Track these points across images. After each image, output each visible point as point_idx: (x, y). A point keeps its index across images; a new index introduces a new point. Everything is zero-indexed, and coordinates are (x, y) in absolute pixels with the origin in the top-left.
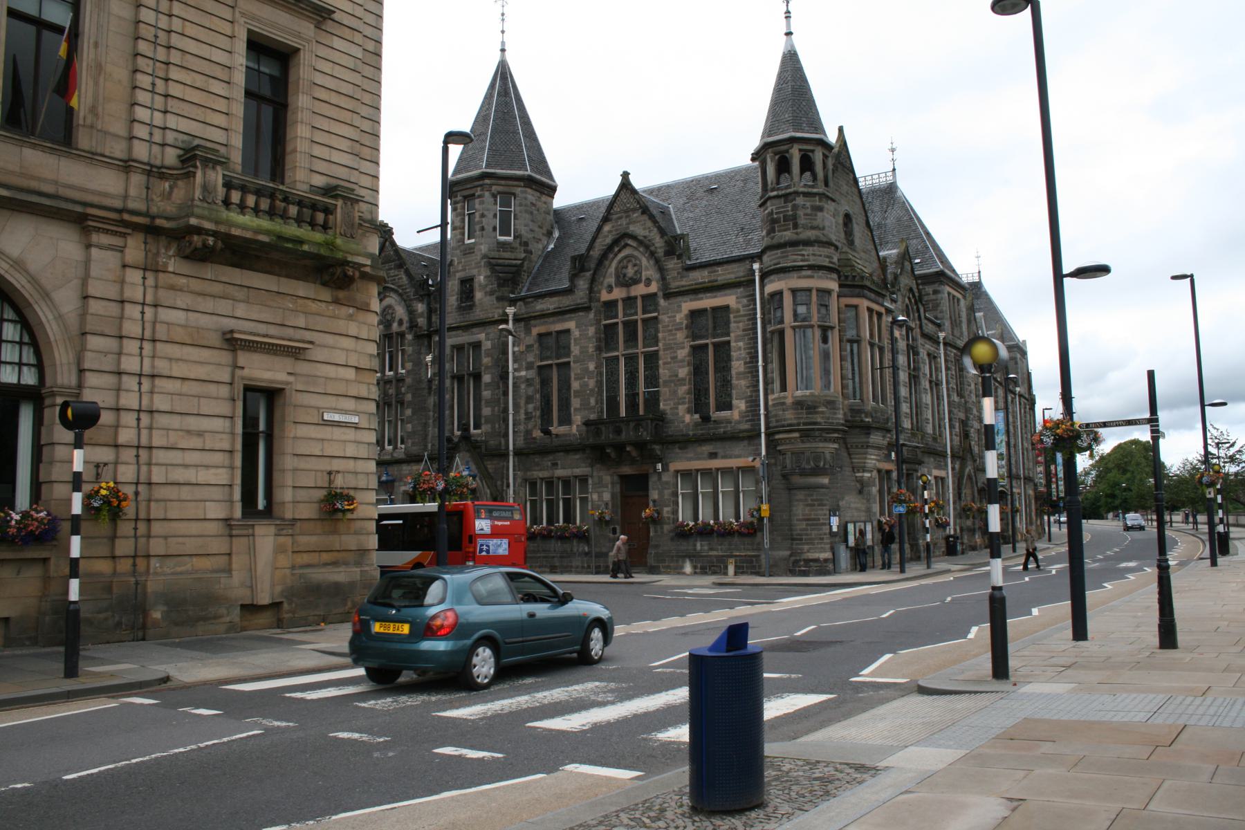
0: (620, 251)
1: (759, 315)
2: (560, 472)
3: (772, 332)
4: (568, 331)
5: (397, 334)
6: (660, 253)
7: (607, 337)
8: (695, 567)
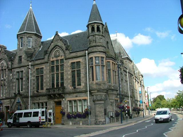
0: (55, 49)
1: (87, 63)
2: (41, 101)
3: (90, 67)
4: (43, 68)
5: (4, 69)
6: (64, 49)
7: (52, 69)
8: (72, 123)
